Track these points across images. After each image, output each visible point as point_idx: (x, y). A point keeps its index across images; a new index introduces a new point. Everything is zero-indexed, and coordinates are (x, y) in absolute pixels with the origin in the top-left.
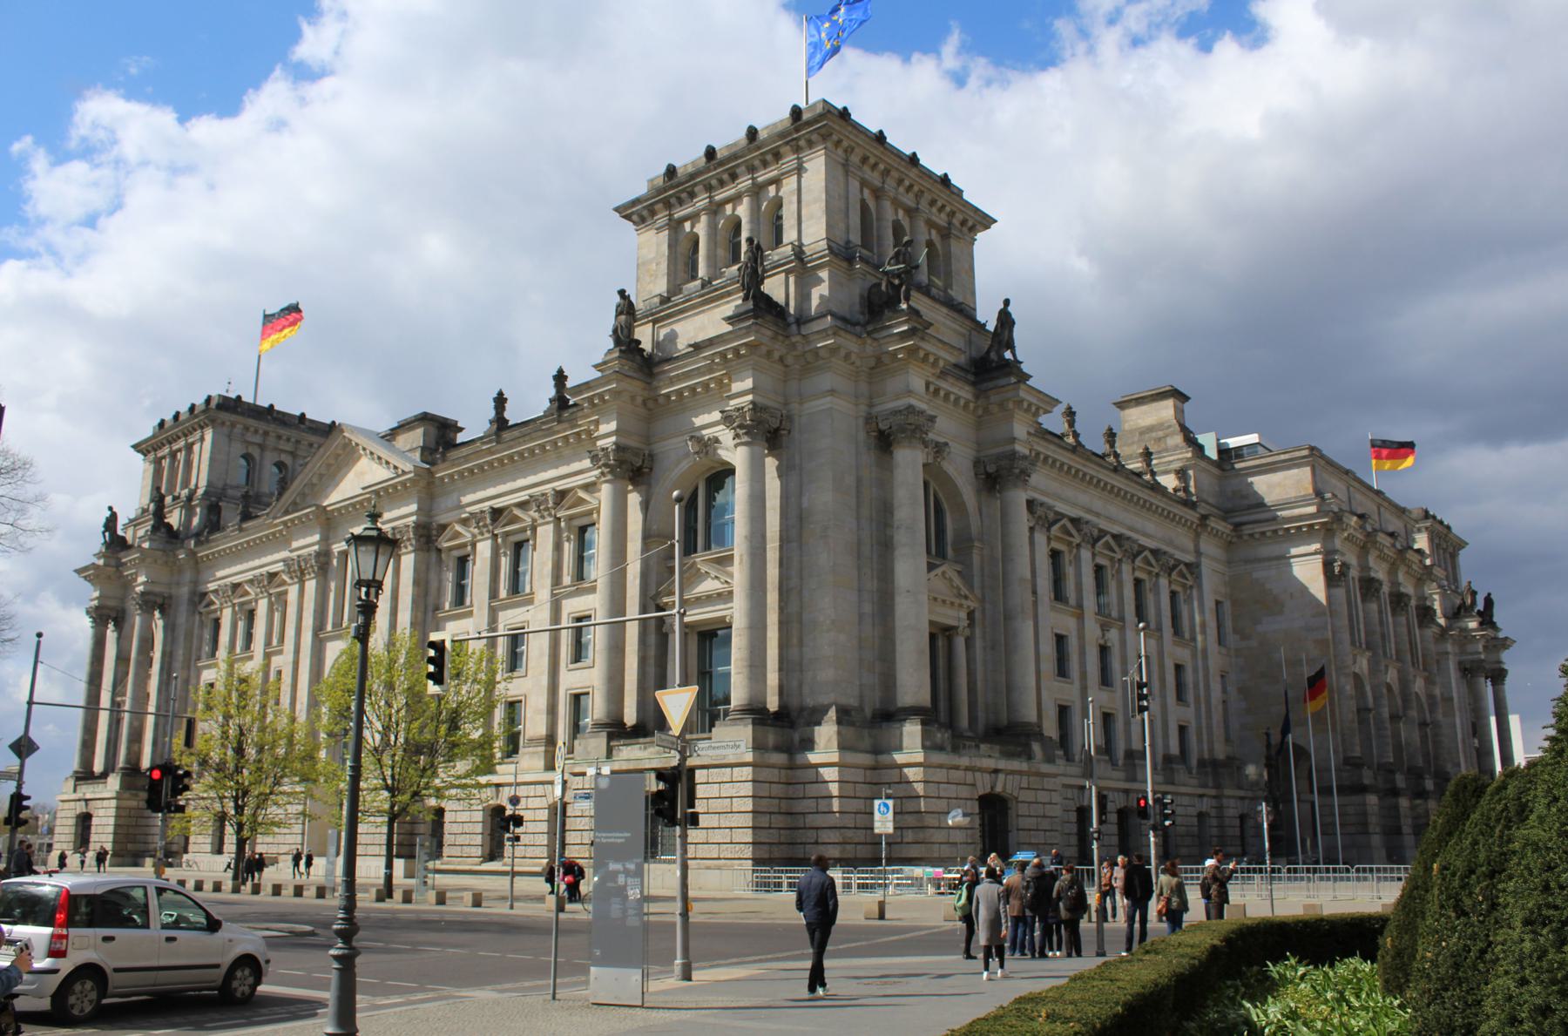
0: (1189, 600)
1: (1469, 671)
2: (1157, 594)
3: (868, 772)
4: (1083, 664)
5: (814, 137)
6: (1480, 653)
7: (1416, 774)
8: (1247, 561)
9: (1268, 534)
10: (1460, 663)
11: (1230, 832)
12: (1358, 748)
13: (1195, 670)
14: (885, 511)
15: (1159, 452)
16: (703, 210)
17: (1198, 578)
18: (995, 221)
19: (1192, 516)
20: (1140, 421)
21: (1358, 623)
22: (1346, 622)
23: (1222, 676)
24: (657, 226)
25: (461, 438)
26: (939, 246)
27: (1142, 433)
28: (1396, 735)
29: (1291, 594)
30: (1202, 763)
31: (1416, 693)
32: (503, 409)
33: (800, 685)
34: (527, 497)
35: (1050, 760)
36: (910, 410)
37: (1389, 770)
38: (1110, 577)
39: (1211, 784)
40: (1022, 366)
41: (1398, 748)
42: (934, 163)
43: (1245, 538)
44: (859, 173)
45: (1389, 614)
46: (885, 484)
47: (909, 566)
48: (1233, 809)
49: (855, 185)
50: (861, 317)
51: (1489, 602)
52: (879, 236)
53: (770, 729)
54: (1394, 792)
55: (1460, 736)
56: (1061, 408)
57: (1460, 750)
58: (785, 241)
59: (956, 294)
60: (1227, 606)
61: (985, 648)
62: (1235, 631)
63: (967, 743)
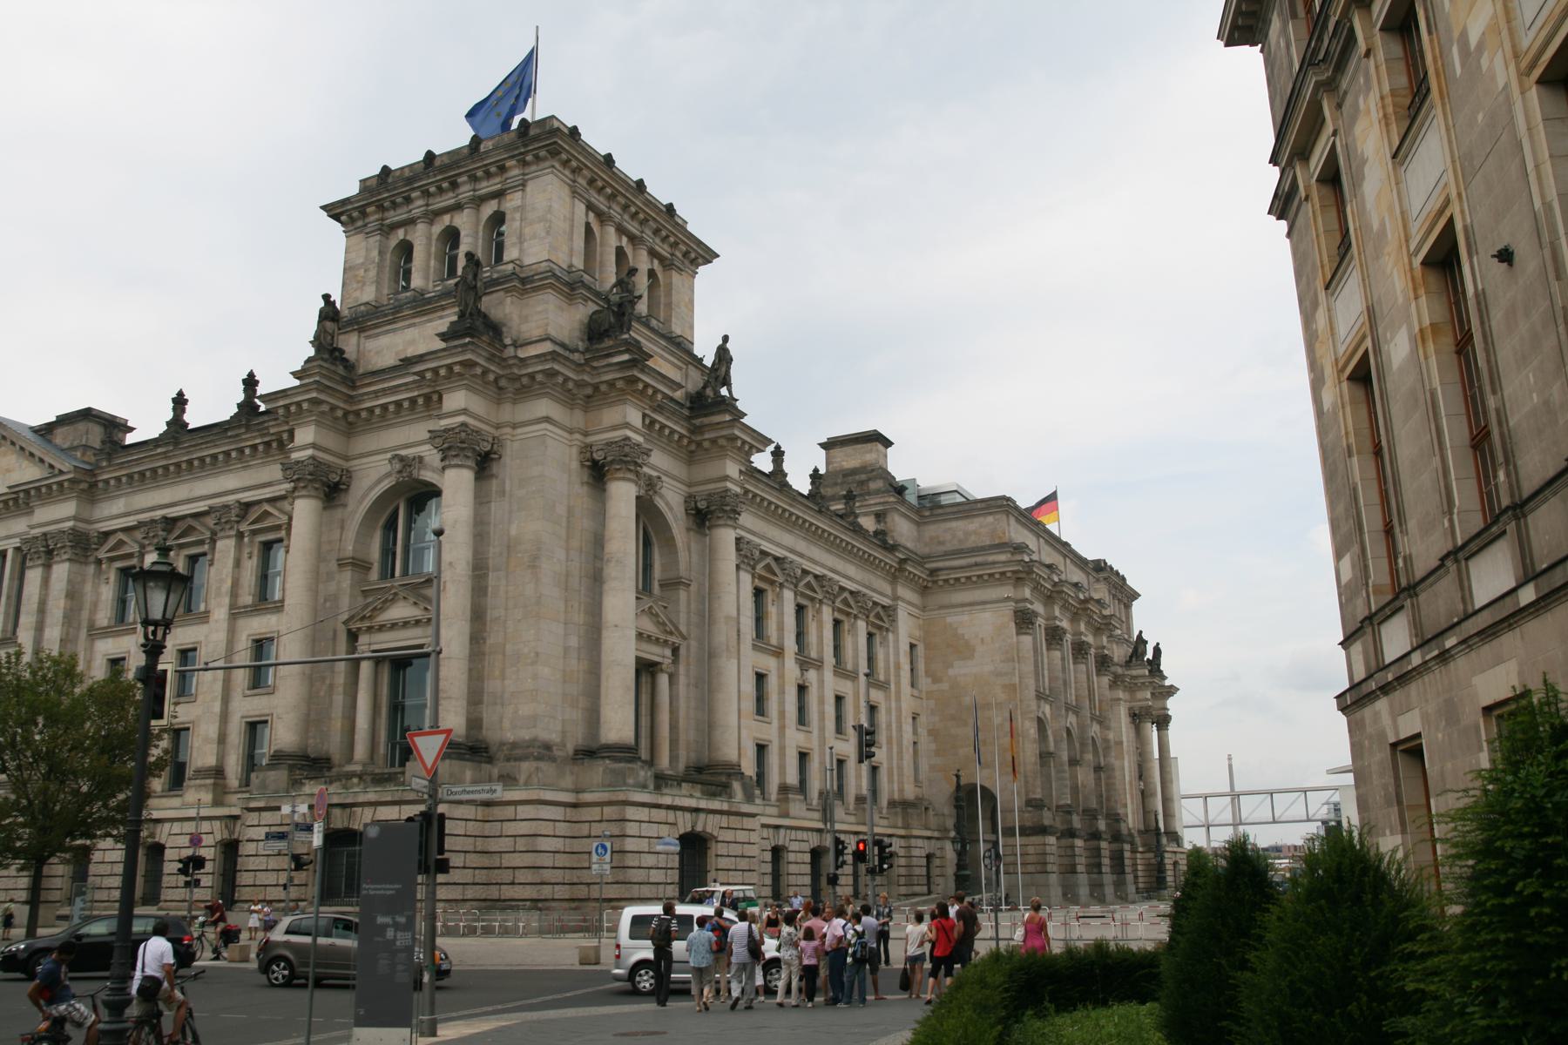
0: (884, 641)
1: (1137, 718)
2: (855, 635)
3: (568, 810)
4: (782, 703)
5: (543, 153)
6: (1147, 700)
7: (1091, 815)
8: (942, 607)
9: (963, 580)
10: (1130, 709)
11: (917, 871)
12: (1039, 790)
13: (889, 711)
14: (598, 542)
15: (861, 495)
16: (419, 218)
17: (894, 621)
18: (718, 256)
19: (890, 560)
20: (844, 463)
21: (1043, 669)
22: (1032, 668)
23: (914, 718)
24: (368, 230)
25: (130, 439)
26: (660, 276)
27: (845, 476)
28: (1074, 777)
29: (982, 640)
30: (892, 804)
31: (1093, 738)
32: (183, 411)
33: (501, 718)
34: (206, 508)
35: (749, 798)
36: (627, 442)
37: (1067, 811)
38: (810, 617)
39: (900, 824)
40: (738, 404)
41: (1075, 790)
42: (660, 191)
43: (941, 583)
44: (586, 196)
45: (1071, 661)
46: (600, 514)
47: (621, 602)
48: (921, 849)
49: (581, 208)
50: (580, 343)
51: (1157, 651)
52: (601, 262)
53: (468, 763)
54: (1071, 833)
56: (771, 448)
57: (1128, 791)
58: (506, 258)
59: (677, 329)
60: (920, 649)
61: (688, 685)
62: (927, 673)
63: (670, 782)
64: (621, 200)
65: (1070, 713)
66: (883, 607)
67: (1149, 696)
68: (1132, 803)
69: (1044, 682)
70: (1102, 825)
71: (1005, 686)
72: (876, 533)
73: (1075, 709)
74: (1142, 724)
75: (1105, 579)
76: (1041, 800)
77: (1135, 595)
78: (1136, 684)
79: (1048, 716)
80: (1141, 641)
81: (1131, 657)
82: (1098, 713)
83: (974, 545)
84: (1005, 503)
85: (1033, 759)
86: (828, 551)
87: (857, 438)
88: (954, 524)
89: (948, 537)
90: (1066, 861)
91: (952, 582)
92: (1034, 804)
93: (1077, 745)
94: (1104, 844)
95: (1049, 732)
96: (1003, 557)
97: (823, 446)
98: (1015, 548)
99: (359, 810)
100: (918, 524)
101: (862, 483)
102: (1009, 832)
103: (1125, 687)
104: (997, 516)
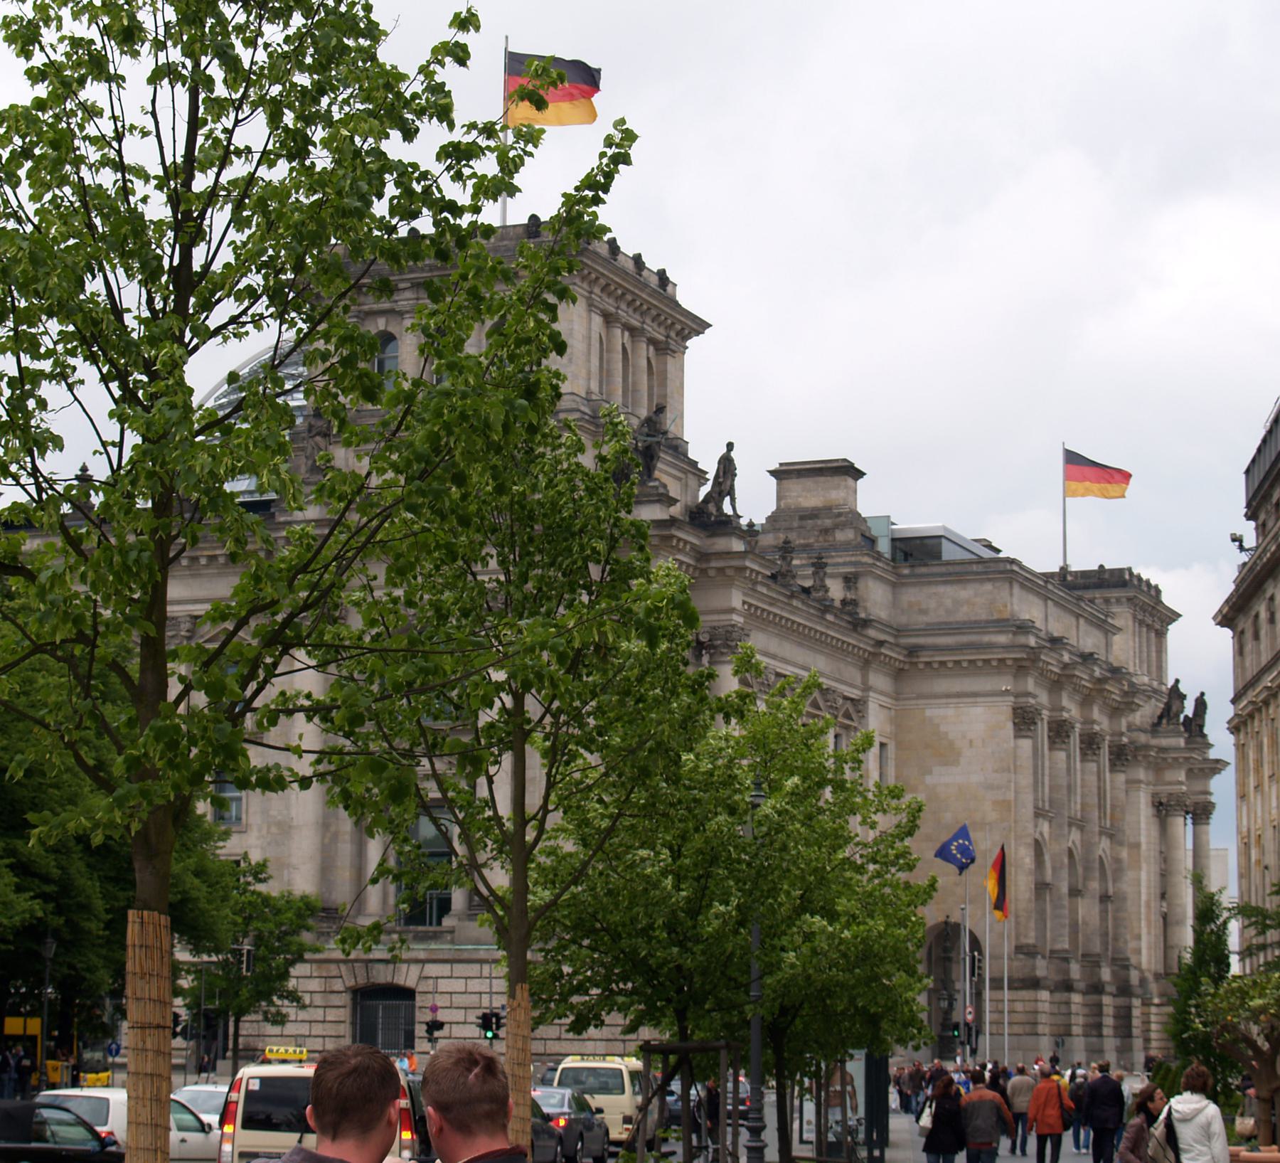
1: (1163, 809)
6: (1181, 783)
7: (1091, 962)
8: (920, 697)
10: (1154, 795)
12: (1032, 934)
16: (407, 312)
21: (1043, 775)
27: (802, 518)
28: (1074, 911)
41: (1074, 927)
43: (921, 666)
45: (1078, 759)
54: (1068, 986)
55: (1144, 897)
57: (1143, 917)
64: (629, 297)
65: (1074, 829)
66: (852, 700)
67: (1182, 777)
68: (1149, 933)
69: (1043, 792)
70: (1106, 974)
71: (995, 803)
72: (844, 602)
73: (1079, 823)
74: (1170, 819)
75: (1129, 599)
76: (1035, 946)
77: (1174, 616)
78: (1164, 759)
79: (1046, 835)
80: (1176, 694)
81: (1161, 717)
82: (1108, 825)
83: (966, 619)
84: (1008, 567)
85: (1027, 895)
86: (800, 645)
87: (821, 469)
88: (941, 589)
89: (932, 604)
90: (1060, 1020)
91: (936, 666)
92: (1023, 950)
93: (1080, 870)
94: (1106, 999)
95: (1047, 858)
96: (1002, 639)
97: (773, 473)
98: (1019, 627)
99: (404, 967)
100: (894, 585)
101: (826, 531)
102: (997, 984)
103: (1149, 763)
104: (998, 584)
